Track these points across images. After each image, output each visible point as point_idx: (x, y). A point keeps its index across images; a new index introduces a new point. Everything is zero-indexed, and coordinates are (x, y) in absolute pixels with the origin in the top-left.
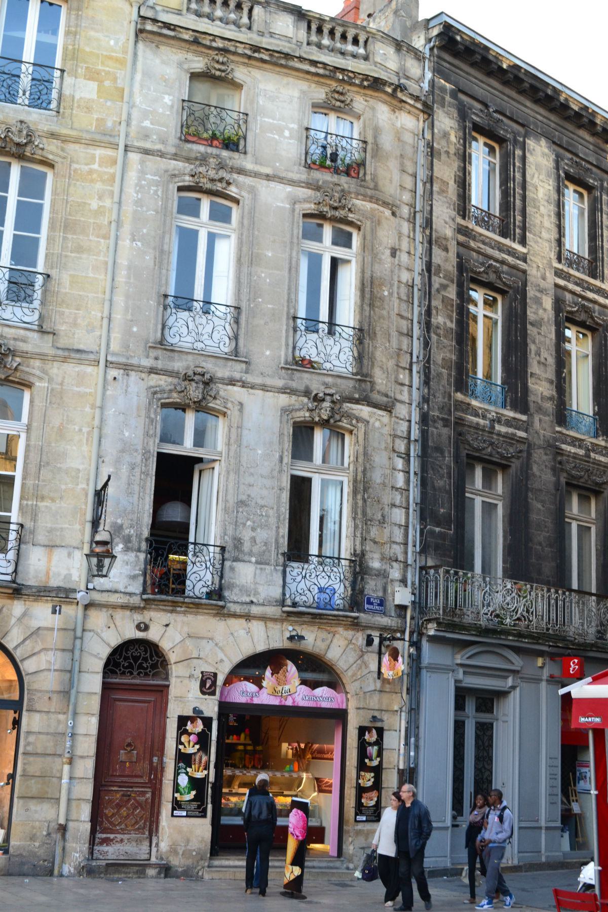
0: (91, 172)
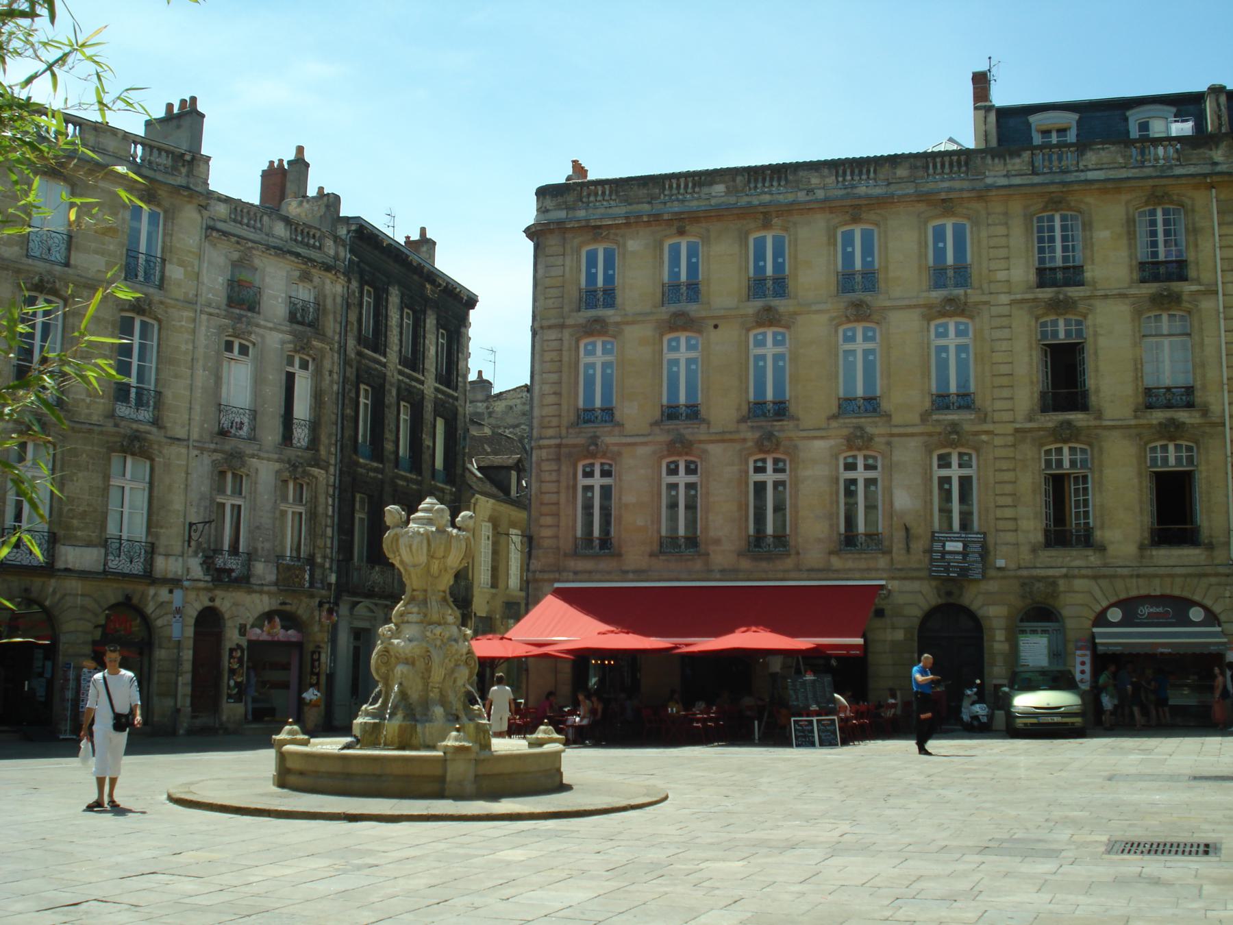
0: (182, 326)
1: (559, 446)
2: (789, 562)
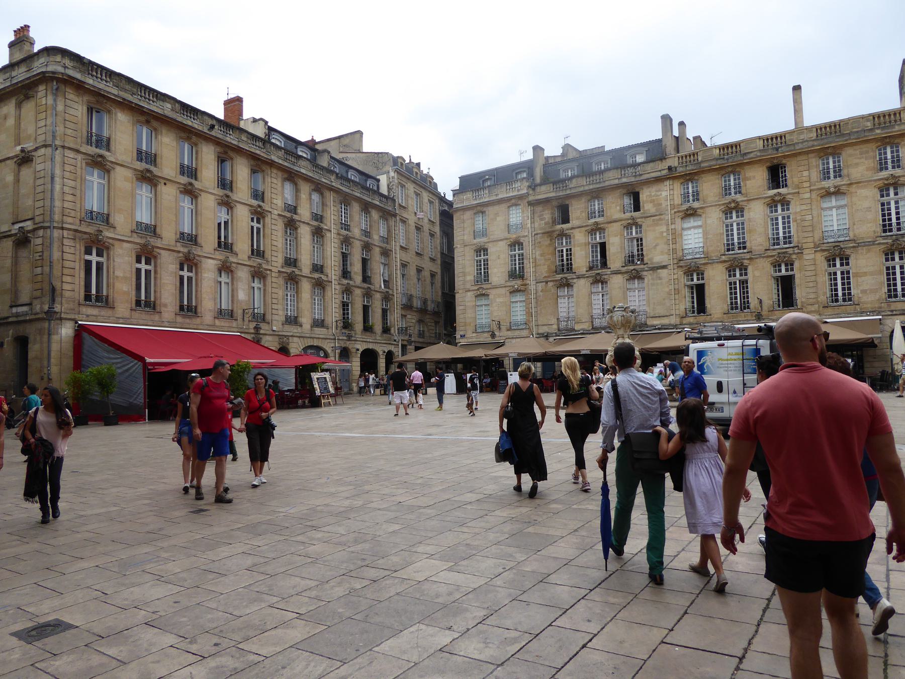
1: (76, 231)
2: (198, 321)
